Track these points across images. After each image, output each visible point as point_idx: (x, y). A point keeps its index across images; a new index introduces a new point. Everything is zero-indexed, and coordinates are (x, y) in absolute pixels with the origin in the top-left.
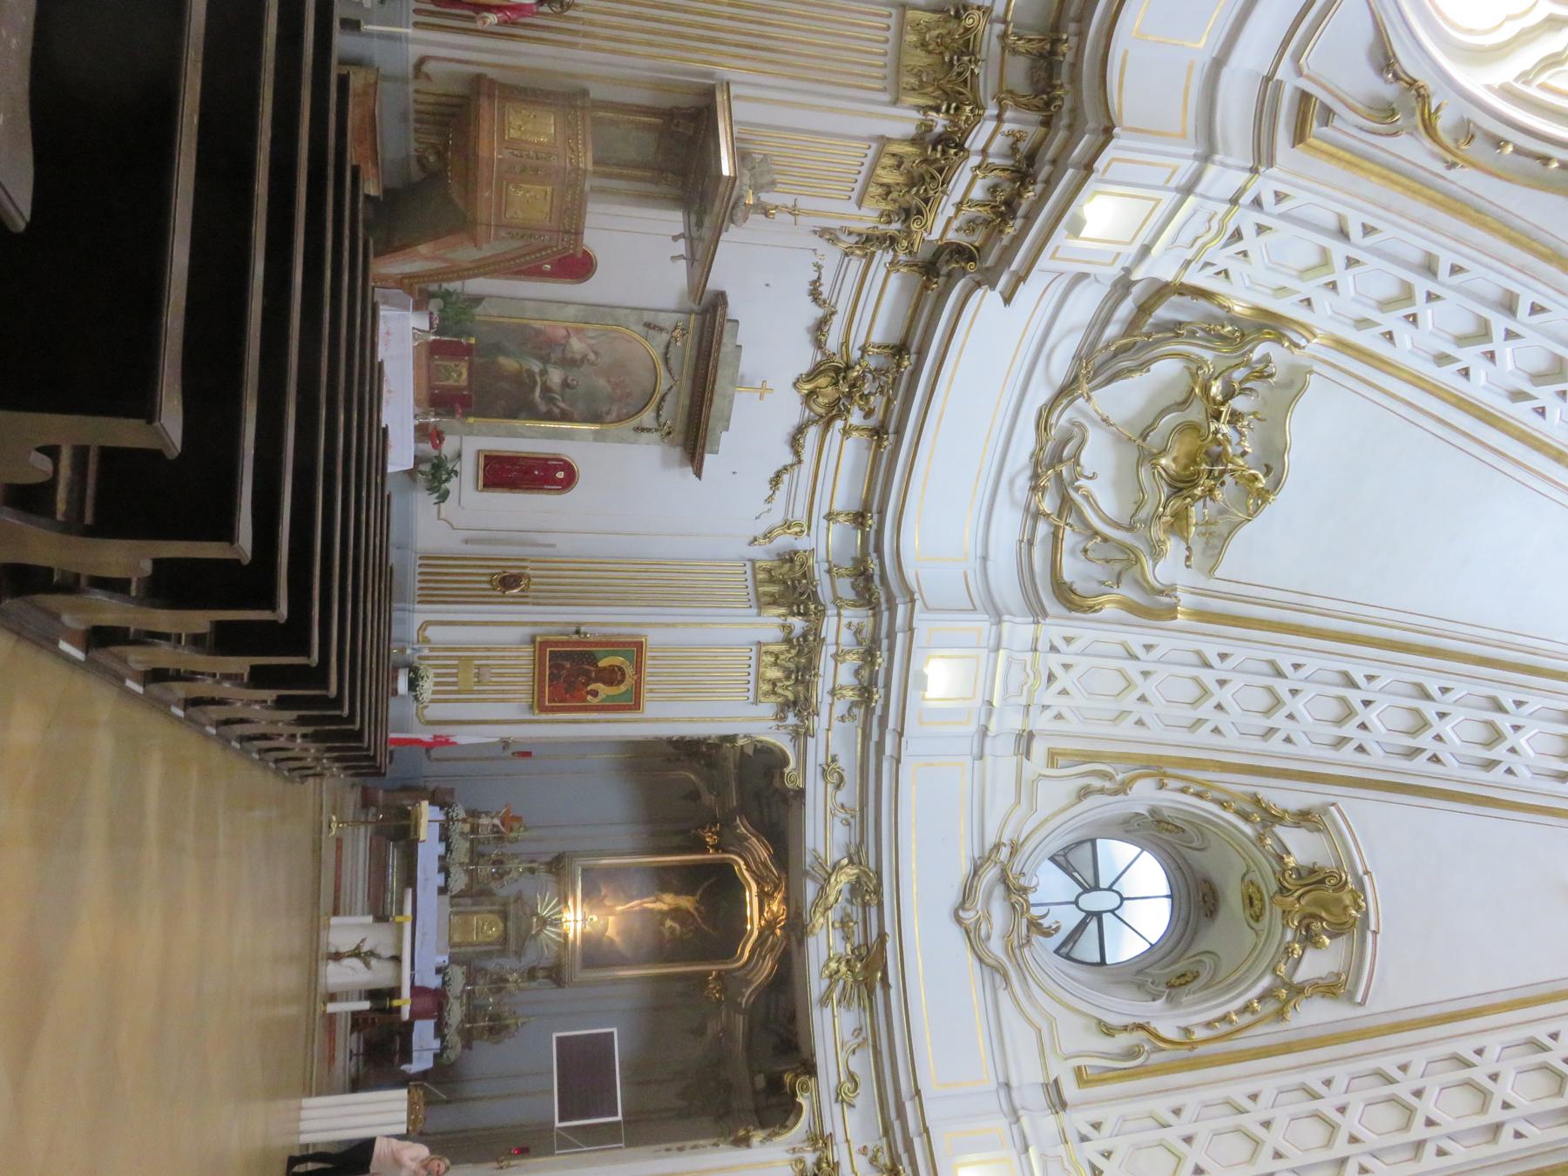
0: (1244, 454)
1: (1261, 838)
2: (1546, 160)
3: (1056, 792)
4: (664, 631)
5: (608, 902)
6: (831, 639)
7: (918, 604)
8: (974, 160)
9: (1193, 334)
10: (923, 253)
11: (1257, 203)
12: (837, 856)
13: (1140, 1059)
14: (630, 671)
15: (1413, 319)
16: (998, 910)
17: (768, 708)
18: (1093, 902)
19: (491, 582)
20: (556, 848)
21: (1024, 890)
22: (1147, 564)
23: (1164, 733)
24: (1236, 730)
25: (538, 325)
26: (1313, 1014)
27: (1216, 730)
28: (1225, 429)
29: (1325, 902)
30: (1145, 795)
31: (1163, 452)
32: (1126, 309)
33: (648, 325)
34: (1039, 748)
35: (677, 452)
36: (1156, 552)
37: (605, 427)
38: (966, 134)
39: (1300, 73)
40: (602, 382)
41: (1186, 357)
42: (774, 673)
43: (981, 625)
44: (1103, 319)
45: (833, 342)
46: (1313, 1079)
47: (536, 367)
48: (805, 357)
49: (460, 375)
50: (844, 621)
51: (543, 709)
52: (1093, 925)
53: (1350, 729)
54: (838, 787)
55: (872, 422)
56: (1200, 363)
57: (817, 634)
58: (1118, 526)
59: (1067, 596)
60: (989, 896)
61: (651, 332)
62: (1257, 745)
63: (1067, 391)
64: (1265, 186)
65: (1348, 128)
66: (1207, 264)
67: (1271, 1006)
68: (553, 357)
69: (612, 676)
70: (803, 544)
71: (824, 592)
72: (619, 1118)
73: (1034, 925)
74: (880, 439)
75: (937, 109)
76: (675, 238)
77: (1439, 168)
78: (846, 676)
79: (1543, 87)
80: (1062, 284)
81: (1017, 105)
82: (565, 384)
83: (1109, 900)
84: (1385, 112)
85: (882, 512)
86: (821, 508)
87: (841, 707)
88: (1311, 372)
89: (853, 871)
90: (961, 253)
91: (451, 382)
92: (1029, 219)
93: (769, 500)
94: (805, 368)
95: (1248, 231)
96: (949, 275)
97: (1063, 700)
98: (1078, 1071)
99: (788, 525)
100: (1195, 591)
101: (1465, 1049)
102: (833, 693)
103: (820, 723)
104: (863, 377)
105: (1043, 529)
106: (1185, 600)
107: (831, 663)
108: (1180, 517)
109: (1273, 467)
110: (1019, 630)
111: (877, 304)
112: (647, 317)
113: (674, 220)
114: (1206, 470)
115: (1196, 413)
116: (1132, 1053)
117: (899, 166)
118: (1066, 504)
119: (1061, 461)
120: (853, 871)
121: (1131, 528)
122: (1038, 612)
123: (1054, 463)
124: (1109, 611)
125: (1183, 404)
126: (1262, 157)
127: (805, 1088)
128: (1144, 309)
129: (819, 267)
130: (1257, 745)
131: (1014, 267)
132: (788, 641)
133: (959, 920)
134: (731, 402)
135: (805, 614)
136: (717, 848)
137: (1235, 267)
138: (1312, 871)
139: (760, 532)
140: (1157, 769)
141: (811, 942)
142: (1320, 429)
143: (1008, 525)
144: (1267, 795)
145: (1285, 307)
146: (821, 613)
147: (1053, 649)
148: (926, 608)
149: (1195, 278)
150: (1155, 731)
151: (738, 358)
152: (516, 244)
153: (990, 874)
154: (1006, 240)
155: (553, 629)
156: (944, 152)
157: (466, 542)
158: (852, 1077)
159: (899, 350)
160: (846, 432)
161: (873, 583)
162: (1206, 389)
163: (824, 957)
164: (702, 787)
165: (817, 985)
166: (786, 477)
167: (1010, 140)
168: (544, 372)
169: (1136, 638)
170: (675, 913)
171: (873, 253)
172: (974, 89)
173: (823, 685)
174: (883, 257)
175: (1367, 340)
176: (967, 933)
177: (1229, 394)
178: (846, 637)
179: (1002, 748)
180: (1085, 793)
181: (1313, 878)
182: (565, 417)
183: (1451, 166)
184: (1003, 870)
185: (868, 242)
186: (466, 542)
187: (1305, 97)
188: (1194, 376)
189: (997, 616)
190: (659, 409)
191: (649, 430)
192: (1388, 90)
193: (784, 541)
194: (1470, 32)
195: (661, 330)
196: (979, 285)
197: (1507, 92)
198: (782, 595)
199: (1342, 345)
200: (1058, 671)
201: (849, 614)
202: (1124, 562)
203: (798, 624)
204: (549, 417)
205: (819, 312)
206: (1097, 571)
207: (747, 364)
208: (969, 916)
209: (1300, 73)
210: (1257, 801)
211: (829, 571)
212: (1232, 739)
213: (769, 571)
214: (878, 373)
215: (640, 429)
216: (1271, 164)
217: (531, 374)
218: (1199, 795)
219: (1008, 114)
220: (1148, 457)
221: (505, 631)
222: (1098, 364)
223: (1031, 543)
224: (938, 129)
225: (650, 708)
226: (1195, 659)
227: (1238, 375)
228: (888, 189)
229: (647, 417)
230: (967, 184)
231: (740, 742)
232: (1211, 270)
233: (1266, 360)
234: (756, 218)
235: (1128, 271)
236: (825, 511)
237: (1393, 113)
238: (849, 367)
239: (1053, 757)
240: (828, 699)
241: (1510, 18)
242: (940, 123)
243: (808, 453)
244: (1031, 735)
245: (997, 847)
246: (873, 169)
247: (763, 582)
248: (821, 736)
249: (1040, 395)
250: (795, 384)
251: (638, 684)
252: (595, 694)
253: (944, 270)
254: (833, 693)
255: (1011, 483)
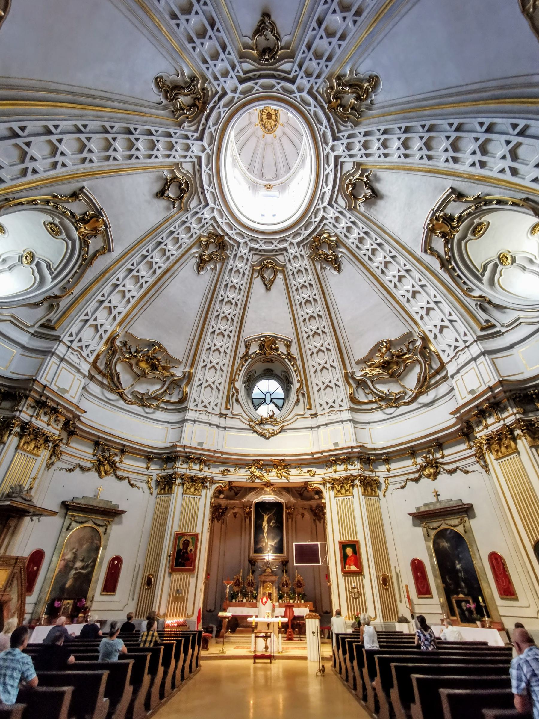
0: (148, 351)
1: (251, 358)
2: (76, 272)
3: (237, 409)
4: (174, 525)
5: (264, 545)
6: (184, 471)
7: (177, 444)
8: (33, 419)
9: (110, 360)
10: (64, 435)
11: (71, 342)
12: (249, 472)
13: (304, 393)
14: (185, 538)
15: (115, 307)
16: (267, 427)
17: (203, 492)
18: (268, 400)
19: (148, 589)
20: (247, 563)
21: (262, 419)
22: (176, 378)
23: (222, 379)
24: (223, 361)
25: (57, 572)
26: (294, 351)
27: (224, 365)
28: (140, 355)
29: (268, 344)
30: (239, 385)
31: (144, 371)
32: (99, 377)
33: (68, 529)
34: (224, 412)
35: (116, 519)
36: (174, 375)
37: (102, 545)
38: (23, 422)
39: (33, 326)
40: (85, 547)
41: (116, 363)
42: (193, 489)
43: (188, 426)
44: (101, 384)
45: (89, 465)
46: (309, 353)
47: (73, 572)
48: (93, 474)
49: (68, 603)
50: (180, 466)
51: (194, 570)
52: (274, 401)
53: (226, 334)
54: (229, 471)
55: (119, 454)
56: (118, 359)
57: (182, 475)
58: (164, 385)
59: (183, 399)
60: (264, 429)
61: (70, 528)
62: (228, 355)
63: (121, 395)
64: (66, 339)
65: (54, 316)
66: (88, 356)
67: (292, 360)
68: (71, 565)
69: (186, 544)
70: (155, 478)
71: (169, 472)
72: (318, 543)
73: (271, 417)
74: (125, 452)
75: (12, 430)
76: (32, 520)
77: (72, 296)
78: (197, 467)
79: (55, 270)
80: (86, 394)
81: (18, 405)
82: (82, 561)
83: (268, 395)
84: (51, 307)
85: (149, 452)
86: (145, 471)
87: (206, 469)
88: (127, 332)
89: (253, 468)
90: (66, 425)
91: (71, 607)
92: (58, 404)
93: (139, 488)
94: (96, 474)
95: (80, 344)
96: (75, 428)
97: (212, 403)
98: (308, 409)
99: (148, 482)
100: (185, 367)
101: (302, 319)
102: (201, 471)
103: (209, 475)
104: (103, 456)
105: (162, 405)
106: (187, 369)
107: (192, 471)
108: (164, 368)
109: (152, 344)
110: (190, 415)
111: (81, 451)
112: (64, 529)
113: (27, 519)
114: (151, 360)
115: (133, 362)
116: (303, 395)
117: (28, 443)
118: (156, 398)
119: (143, 398)
120: (253, 468)
121: (165, 382)
122: (186, 409)
123: (143, 401)
124: (188, 390)
125: (131, 366)
126: (57, 339)
127: (311, 485)
128: (100, 372)
129: (62, 469)
130: (228, 355)
131: (74, 410)
132: (183, 484)
133: (269, 438)
134: (102, 500)
135: (176, 478)
136: (250, 508)
137: (90, 348)
138: (260, 346)
139: (149, 492)
140: (232, 381)
141: (272, 481)
142: (142, 331)
143: (160, 415)
144: (241, 356)
145: (105, 337)
146: (175, 473)
147: (197, 405)
148: (179, 441)
149: (91, 359)
150: (222, 380)
151: (87, 497)
152: (15, 582)
153: (257, 428)
154: (64, 411)
155: (168, 565)
156: (27, 429)
157: (133, 599)
158: (308, 471)
159: (97, 444)
160: (121, 462)
161: (169, 457)
162: (127, 358)
163: (276, 478)
164: (233, 511)
165: (284, 480)
166: (132, 482)
167: (30, 408)
168: (76, 569)
169: (197, 383)
170: (269, 522)
171: (61, 451)
172: (8, 418)
173: (199, 475)
174: (63, 447)
175: (119, 319)
176: (272, 436)
177: (130, 353)
178: (185, 466)
179: (223, 422)
180: (237, 401)
181: (262, 347)
182: (95, 561)
183: (72, 293)
184: (257, 424)
185: (55, 452)
186: (133, 599)
187: (42, 326)
188: (122, 361)
189: (185, 421)
190: (99, 526)
191: (106, 529)
192: (46, 305)
193: (153, 484)
194: (34, 284)
195: (70, 525)
196: (79, 419)
197: (54, 279)
198: (169, 485)
199: (120, 324)
200: (203, 404)
201: (178, 465)
202: (176, 384)
203: (179, 481)
204: (93, 567)
205: (78, 469)
206: (176, 391)
207: (90, 494)
208: (268, 435)
209: (33, 326)
210: (242, 358)
211: (164, 470)
212: (226, 361)
213: (161, 489)
214: (103, 451)
215: (105, 533)
216: (59, 337)
217: (75, 574)
218: (240, 371)
219: (20, 409)
220: (144, 375)
221: (165, 583)
222: (114, 385)
223: (166, 409)
224: (19, 430)
225: (198, 530)
226: (203, 369)
227: (124, 349)
228: (36, 447)
229: (101, 530)
230: (41, 422)
231: (213, 501)
232: (90, 355)
233: (121, 342)
234: (32, 493)
235: (85, 376)
236: (146, 470)
237: (52, 305)
238: (99, 460)
239: (227, 408)
240: (203, 473)
241: (33, 274)
242: (17, 429)
243: (126, 475)
244: (221, 413)
245: (250, 425)
246: (28, 452)
247: (164, 491)
248: (213, 475)
249: (121, 403)
250: (101, 478)
251: (190, 535)
252: (191, 550)
253: (72, 429)
254: (201, 471)
255: (147, 413)
